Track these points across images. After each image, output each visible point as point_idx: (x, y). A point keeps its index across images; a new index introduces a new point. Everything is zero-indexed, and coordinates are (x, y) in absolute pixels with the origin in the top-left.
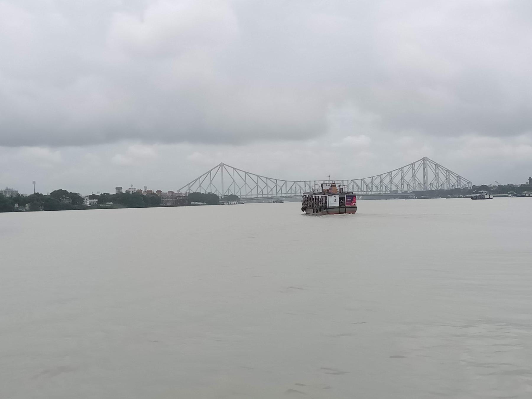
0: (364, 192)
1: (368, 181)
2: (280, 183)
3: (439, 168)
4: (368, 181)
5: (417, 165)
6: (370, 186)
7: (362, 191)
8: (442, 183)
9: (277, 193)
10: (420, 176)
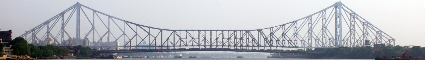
0: (262, 47)
1: (267, 33)
4: (267, 33)
7: (259, 46)
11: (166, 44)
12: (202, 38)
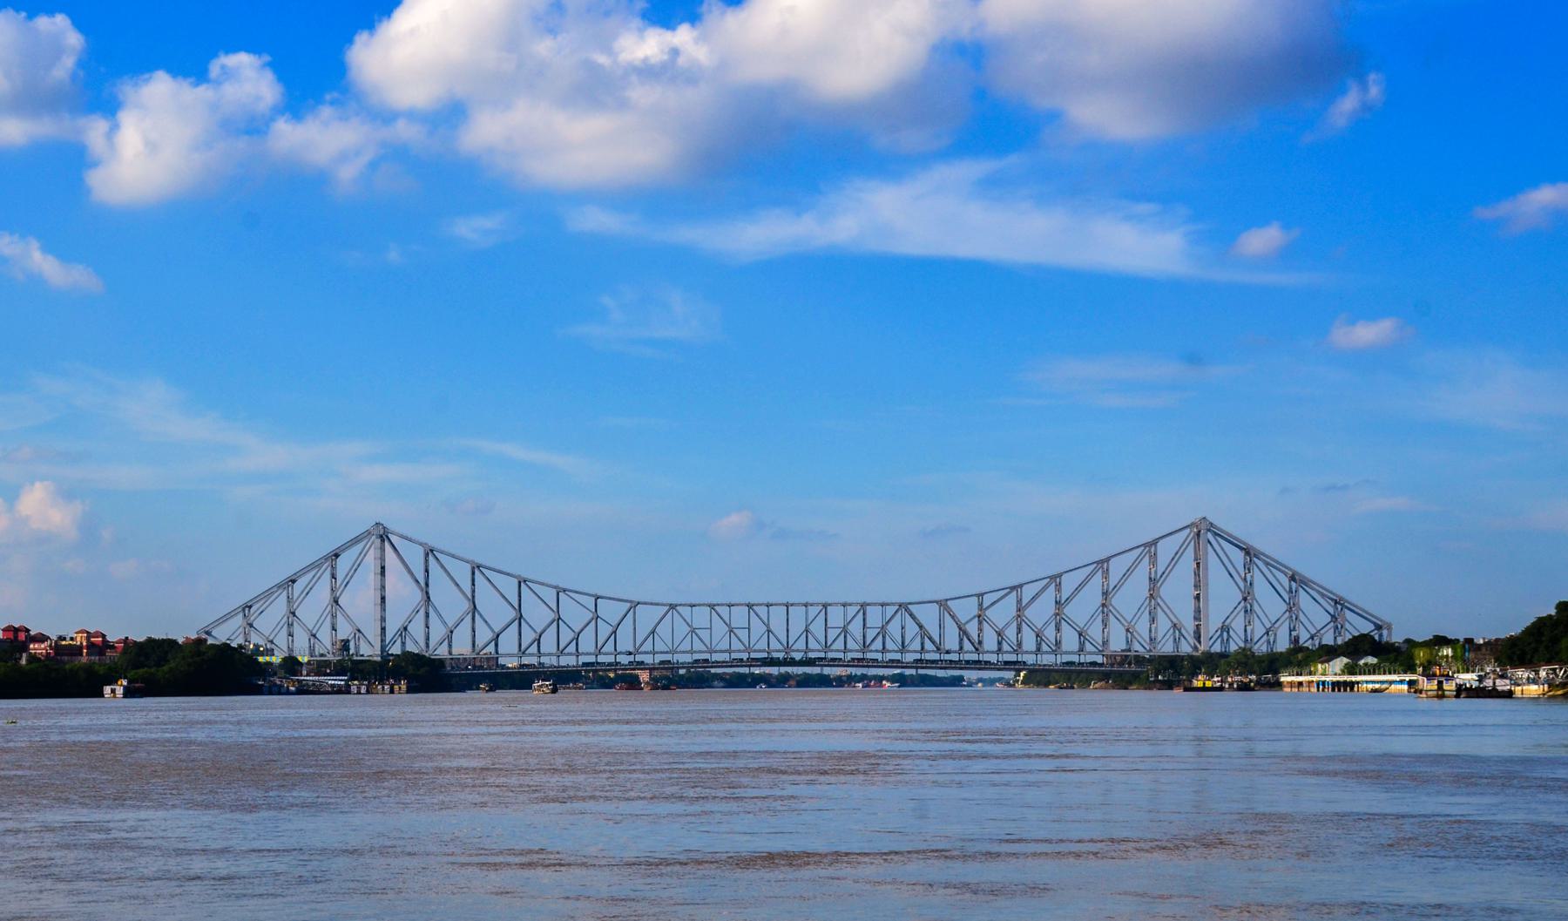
0: (948, 652)
1: (966, 610)
2: (611, 612)
3: (1255, 559)
4: (966, 610)
5: (1165, 550)
6: (972, 629)
8: (1268, 626)
9: (561, 652)
10: (1177, 592)
11: (648, 646)
12: (758, 628)
